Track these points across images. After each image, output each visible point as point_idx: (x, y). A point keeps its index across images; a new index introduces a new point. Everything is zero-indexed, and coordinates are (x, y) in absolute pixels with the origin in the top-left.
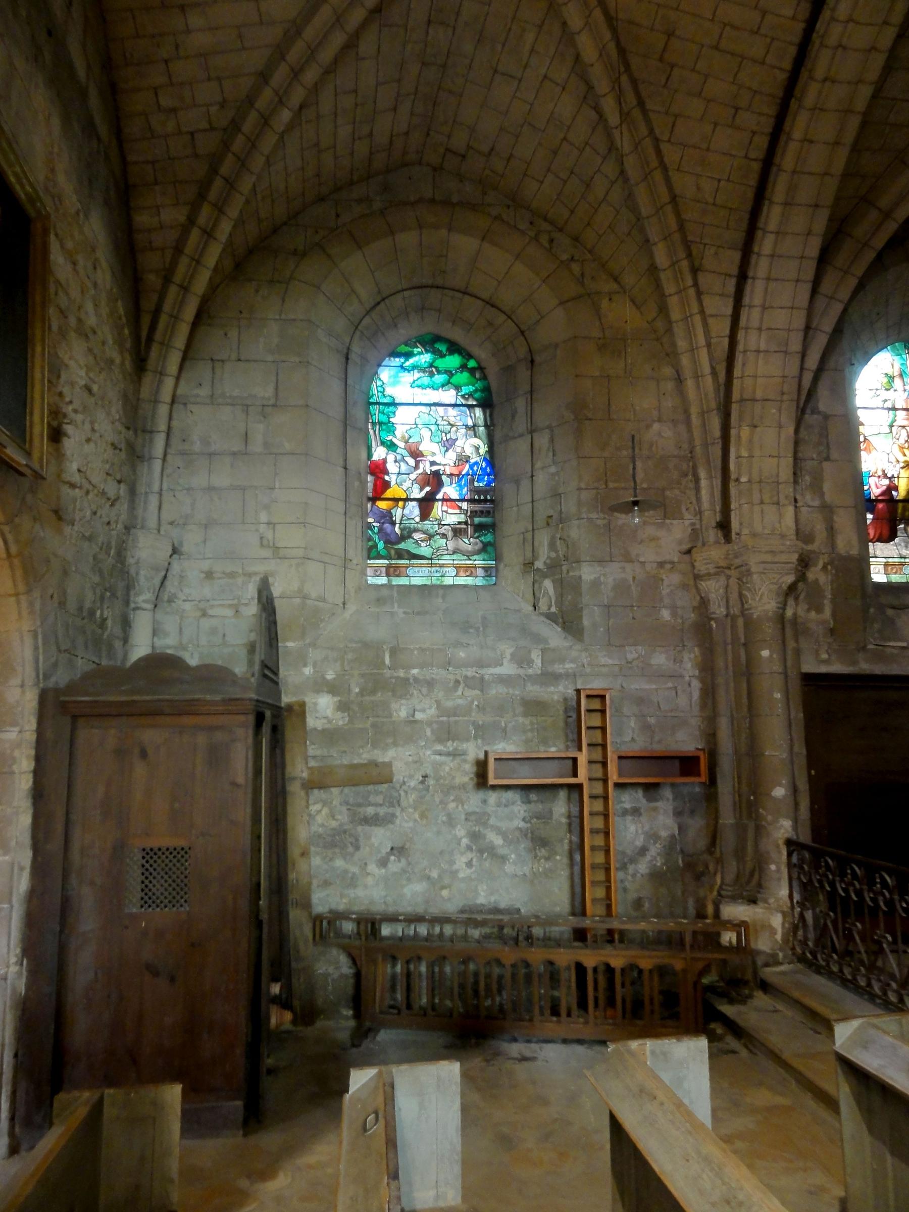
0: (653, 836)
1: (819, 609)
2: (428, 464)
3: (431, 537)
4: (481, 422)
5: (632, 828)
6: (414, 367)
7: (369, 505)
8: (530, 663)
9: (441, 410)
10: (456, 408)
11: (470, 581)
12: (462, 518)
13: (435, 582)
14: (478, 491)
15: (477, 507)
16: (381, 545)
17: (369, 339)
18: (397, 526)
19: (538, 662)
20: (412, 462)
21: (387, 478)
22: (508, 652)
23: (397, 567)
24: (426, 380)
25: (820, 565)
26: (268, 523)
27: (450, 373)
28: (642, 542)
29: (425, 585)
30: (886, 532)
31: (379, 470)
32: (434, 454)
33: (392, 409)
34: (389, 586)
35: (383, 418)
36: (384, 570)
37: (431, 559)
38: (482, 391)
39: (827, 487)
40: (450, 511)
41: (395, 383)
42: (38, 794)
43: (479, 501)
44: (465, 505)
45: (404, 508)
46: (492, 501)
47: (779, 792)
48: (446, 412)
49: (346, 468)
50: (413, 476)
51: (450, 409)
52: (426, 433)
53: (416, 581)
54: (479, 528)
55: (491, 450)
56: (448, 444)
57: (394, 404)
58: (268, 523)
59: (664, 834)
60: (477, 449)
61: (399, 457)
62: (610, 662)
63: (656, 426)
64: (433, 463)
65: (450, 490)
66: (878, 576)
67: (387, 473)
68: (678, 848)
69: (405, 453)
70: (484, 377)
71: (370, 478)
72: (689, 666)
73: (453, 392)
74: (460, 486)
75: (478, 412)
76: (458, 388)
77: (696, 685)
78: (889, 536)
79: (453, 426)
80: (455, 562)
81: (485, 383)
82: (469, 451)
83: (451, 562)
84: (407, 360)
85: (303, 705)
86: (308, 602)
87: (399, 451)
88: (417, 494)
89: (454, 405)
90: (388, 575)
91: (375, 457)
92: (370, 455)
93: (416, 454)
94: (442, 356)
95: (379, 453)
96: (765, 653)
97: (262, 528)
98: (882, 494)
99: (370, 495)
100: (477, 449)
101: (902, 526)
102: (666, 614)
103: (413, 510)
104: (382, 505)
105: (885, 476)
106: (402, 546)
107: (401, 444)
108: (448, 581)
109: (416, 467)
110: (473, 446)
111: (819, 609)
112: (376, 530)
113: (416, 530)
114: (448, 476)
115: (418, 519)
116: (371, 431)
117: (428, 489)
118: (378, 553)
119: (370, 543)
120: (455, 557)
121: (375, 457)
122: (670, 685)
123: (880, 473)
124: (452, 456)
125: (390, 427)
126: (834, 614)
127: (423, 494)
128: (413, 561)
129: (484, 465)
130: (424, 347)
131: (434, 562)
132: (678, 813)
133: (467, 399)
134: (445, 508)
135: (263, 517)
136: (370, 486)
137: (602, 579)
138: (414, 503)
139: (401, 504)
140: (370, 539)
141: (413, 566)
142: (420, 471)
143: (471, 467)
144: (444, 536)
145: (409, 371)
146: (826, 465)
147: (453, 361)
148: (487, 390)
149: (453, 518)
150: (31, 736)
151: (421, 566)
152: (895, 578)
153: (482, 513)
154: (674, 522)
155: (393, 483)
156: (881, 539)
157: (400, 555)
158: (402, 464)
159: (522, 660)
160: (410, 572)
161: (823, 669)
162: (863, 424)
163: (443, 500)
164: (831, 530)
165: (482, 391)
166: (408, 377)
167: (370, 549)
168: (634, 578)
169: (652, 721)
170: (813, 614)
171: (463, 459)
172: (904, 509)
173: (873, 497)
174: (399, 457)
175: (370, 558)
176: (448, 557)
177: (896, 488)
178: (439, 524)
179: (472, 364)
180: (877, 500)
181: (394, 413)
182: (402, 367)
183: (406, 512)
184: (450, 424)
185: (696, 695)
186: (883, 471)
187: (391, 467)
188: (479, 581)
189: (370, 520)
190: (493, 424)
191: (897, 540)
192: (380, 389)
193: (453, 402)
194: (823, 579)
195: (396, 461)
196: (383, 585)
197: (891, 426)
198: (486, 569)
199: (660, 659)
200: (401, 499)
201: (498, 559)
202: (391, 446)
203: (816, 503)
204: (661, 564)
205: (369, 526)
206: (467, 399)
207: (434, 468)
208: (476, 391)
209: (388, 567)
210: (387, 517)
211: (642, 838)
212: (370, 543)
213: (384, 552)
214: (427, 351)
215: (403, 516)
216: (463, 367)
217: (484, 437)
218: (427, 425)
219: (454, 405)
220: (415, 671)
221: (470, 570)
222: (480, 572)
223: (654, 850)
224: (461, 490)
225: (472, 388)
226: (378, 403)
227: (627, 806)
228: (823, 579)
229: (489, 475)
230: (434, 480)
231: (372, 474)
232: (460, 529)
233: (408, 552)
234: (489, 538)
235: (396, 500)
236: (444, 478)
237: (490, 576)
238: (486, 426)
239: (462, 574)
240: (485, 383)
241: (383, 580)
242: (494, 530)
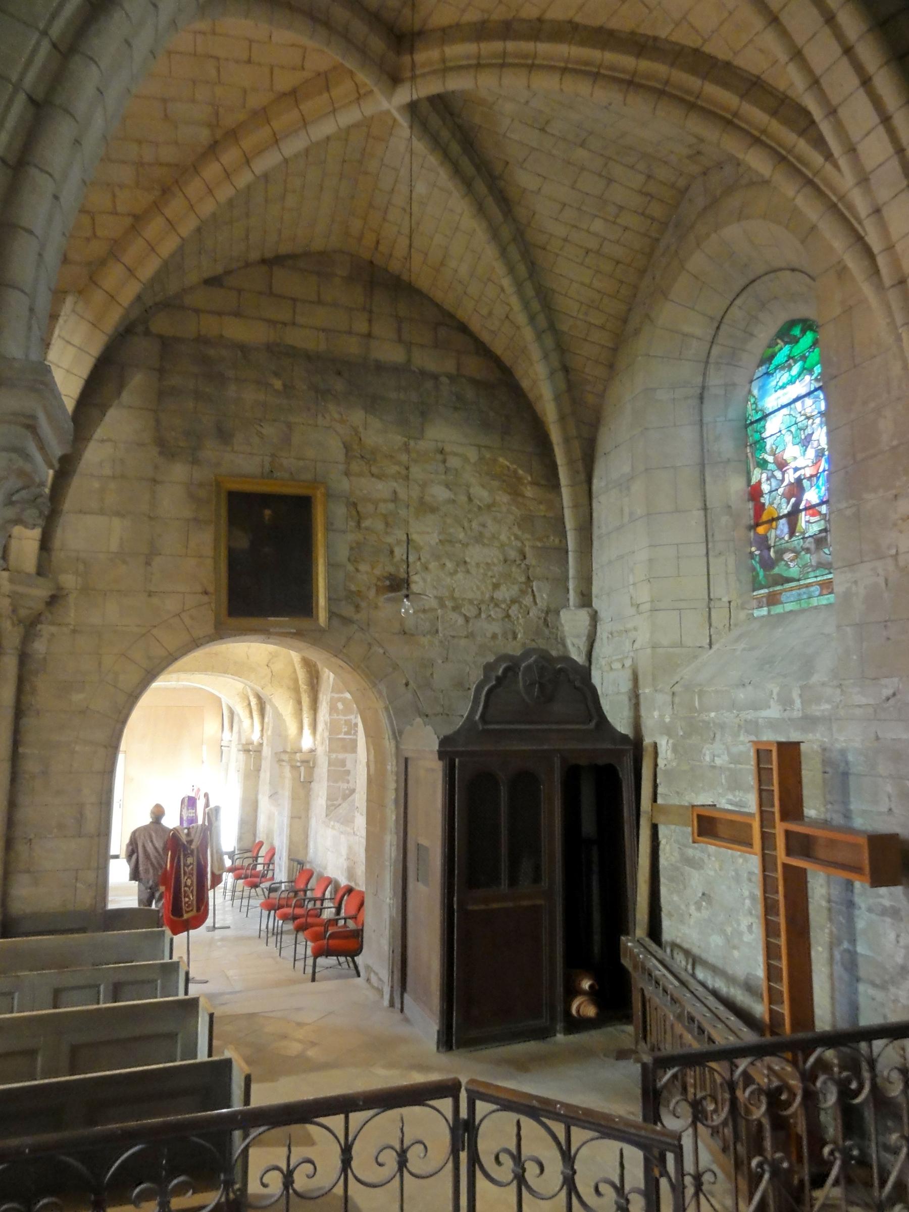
2: (791, 471)
3: (797, 553)
6: (776, 368)
8: (792, 703)
10: (812, 396)
17: (728, 364)
18: (772, 550)
19: (798, 703)
22: (776, 690)
27: (804, 358)
37: (799, 580)
40: (813, 519)
50: (781, 491)
51: (806, 399)
62: (864, 701)
64: (796, 469)
65: (812, 496)
74: (818, 487)
80: (819, 579)
83: (815, 580)
86: (660, 651)
104: (761, 530)
107: (770, 459)
109: (783, 480)
112: (757, 559)
115: (786, 538)
117: (793, 500)
118: (760, 584)
120: (818, 573)
127: (789, 508)
131: (802, 582)
134: (808, 518)
137: (854, 589)
141: (785, 590)
144: (808, 550)
151: (791, 589)
158: (772, 480)
159: (786, 702)
163: (806, 509)
168: (886, 581)
175: (754, 591)
176: (812, 574)
178: (803, 538)
187: (765, 488)
189: (753, 549)
192: (754, 406)
215: (776, 537)
220: (713, 714)
227: (887, 903)
232: (822, 538)
233: (780, 576)
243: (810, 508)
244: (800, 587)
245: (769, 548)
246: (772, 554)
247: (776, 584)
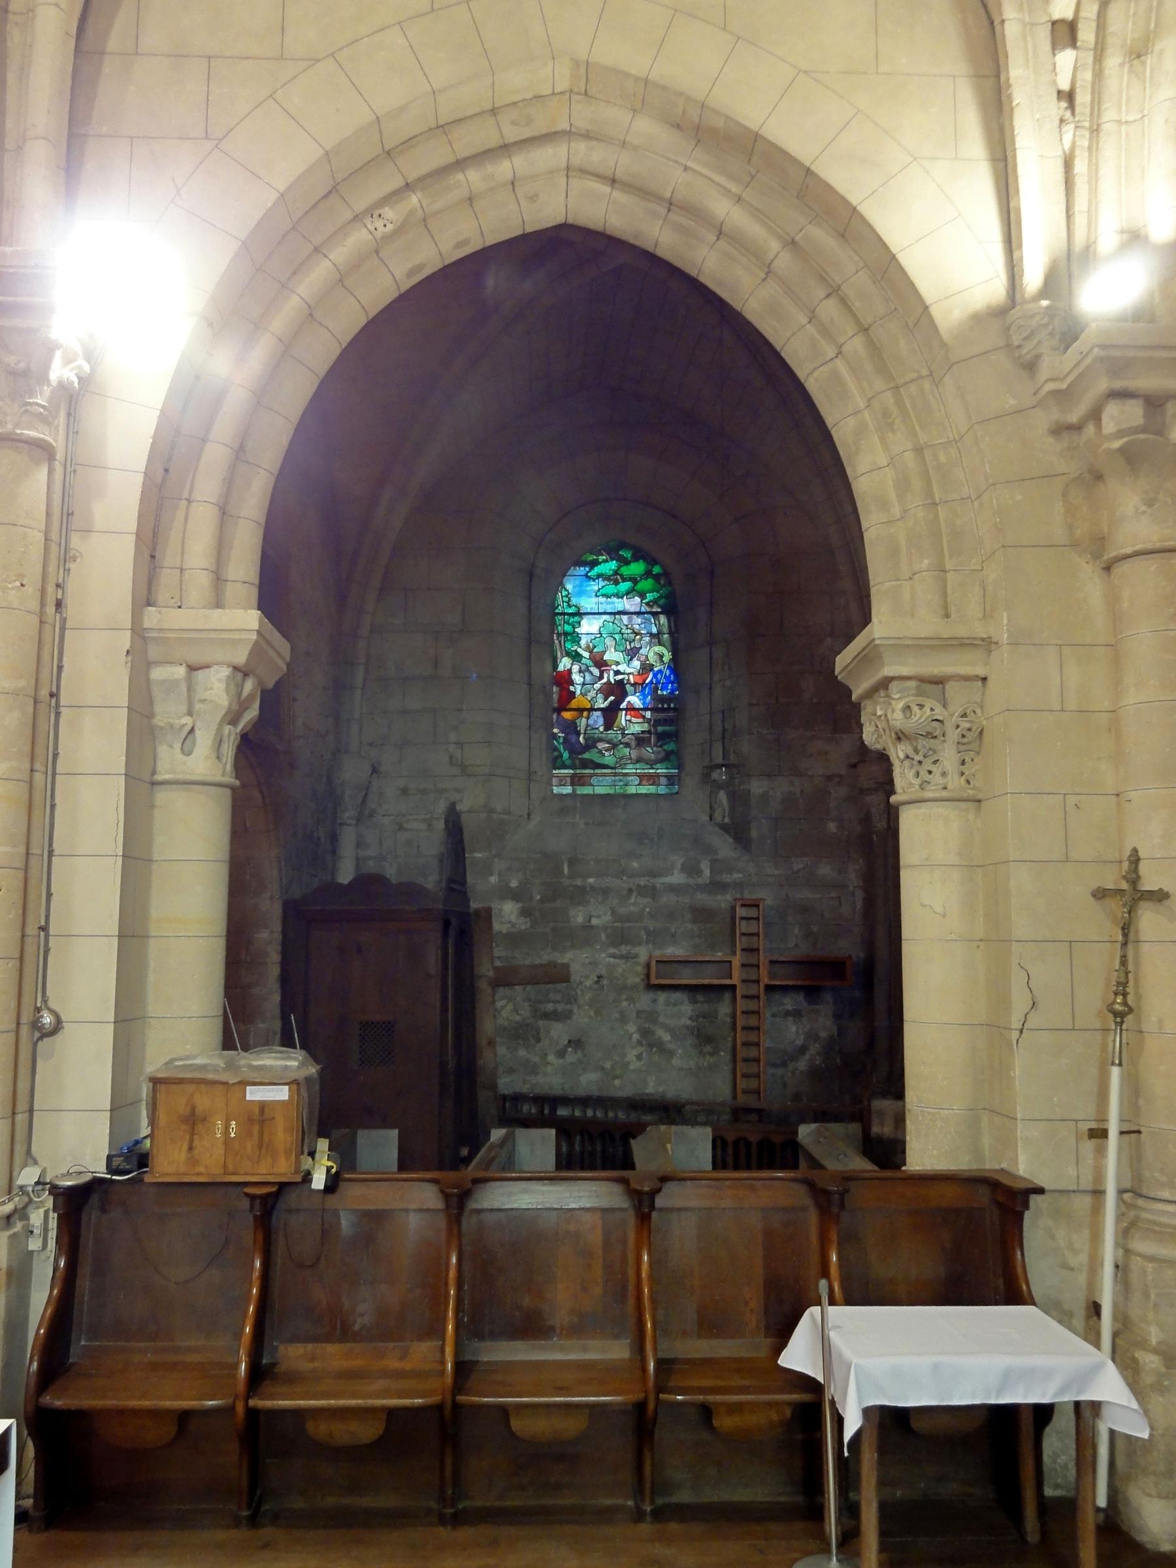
0: (812, 1036)
3: (614, 746)
4: (666, 629)
5: (794, 1029)
6: (599, 576)
7: (555, 716)
8: (699, 872)
9: (625, 618)
11: (652, 789)
12: (646, 727)
13: (619, 790)
14: (662, 699)
15: (661, 716)
16: (566, 755)
19: (707, 872)
20: (596, 672)
21: (572, 688)
22: (680, 862)
23: (582, 776)
24: (611, 589)
26: (457, 743)
27: (634, 581)
28: (811, 755)
29: (608, 795)
31: (565, 680)
32: (618, 663)
33: (576, 619)
34: (573, 795)
35: (568, 628)
36: (569, 780)
37: (614, 768)
38: (666, 597)
40: (634, 720)
41: (581, 593)
42: (284, 980)
43: (663, 710)
44: (648, 714)
45: (588, 718)
46: (675, 709)
48: (630, 620)
49: (529, 684)
50: (597, 686)
51: (635, 617)
52: (609, 642)
53: (600, 790)
54: (662, 737)
55: (675, 659)
56: (632, 653)
57: (579, 614)
58: (457, 743)
59: (823, 1034)
60: (661, 656)
61: (583, 668)
62: (776, 872)
63: (828, 641)
64: (617, 673)
65: (634, 700)
67: (572, 683)
68: (837, 1048)
69: (589, 663)
70: (669, 583)
71: (555, 689)
72: (853, 878)
73: (637, 599)
75: (663, 619)
76: (642, 595)
77: (860, 895)
79: (637, 634)
81: (669, 589)
82: (652, 659)
84: (592, 569)
85: (489, 911)
86: (495, 816)
87: (584, 661)
88: (601, 703)
89: (638, 613)
90: (572, 784)
91: (561, 668)
92: (555, 666)
93: (601, 664)
94: (626, 562)
95: (564, 663)
97: (452, 748)
99: (556, 705)
100: (661, 656)
102: (832, 827)
103: (597, 719)
104: (567, 715)
106: (586, 756)
108: (632, 790)
109: (601, 677)
110: (656, 654)
112: (561, 740)
113: (601, 740)
114: (632, 685)
115: (601, 729)
116: (556, 642)
117: (612, 698)
118: (563, 762)
119: (556, 754)
120: (638, 766)
121: (561, 668)
122: (834, 894)
124: (636, 664)
125: (576, 638)
127: (607, 703)
128: (598, 771)
129: (668, 673)
130: (609, 554)
132: (838, 1016)
133: (651, 607)
134: (628, 717)
135: (453, 737)
136: (555, 697)
137: (771, 793)
138: (599, 713)
139: (585, 714)
140: (556, 749)
141: (594, 775)
142: (605, 680)
143: (655, 676)
144: (627, 745)
145: (594, 580)
147: (637, 568)
148: (671, 596)
149: (636, 728)
150: (278, 936)
151: (604, 775)
153: (665, 722)
154: (844, 736)
155: (578, 692)
157: (586, 764)
159: (692, 869)
160: (594, 780)
163: (627, 710)
165: (666, 597)
166: (594, 586)
167: (555, 759)
168: (802, 792)
169: (815, 929)
171: (646, 668)
174: (583, 668)
175: (555, 769)
176: (631, 766)
179: (657, 570)
181: (579, 623)
182: (586, 576)
183: (591, 722)
184: (634, 632)
185: (859, 905)
187: (577, 678)
188: (662, 790)
189: (555, 730)
190: (677, 632)
192: (566, 599)
193: (638, 610)
195: (580, 671)
196: (567, 795)
198: (669, 777)
199: (825, 870)
200: (586, 709)
201: (680, 767)
202: (576, 657)
204: (829, 778)
205: (554, 736)
206: (651, 607)
207: (620, 677)
208: (660, 598)
209: (573, 777)
210: (571, 728)
211: (802, 1037)
212: (556, 754)
213: (568, 762)
214: (612, 559)
215: (587, 725)
216: (648, 574)
217: (668, 644)
218: (611, 635)
219: (638, 613)
220: (591, 880)
221: (653, 779)
222: (663, 780)
223: (814, 1049)
224: (645, 697)
225: (656, 595)
226: (564, 614)
227: (790, 1008)
229: (672, 683)
230: (618, 690)
231: (558, 684)
233: (592, 761)
234: (671, 746)
235: (581, 710)
236: (628, 687)
237: (672, 784)
238: (670, 633)
239: (644, 782)
240: (669, 589)
241: (568, 790)
242: (677, 737)
243: (631, 709)
244: (615, 775)
245: (579, 734)
246: (581, 739)
247: (585, 767)
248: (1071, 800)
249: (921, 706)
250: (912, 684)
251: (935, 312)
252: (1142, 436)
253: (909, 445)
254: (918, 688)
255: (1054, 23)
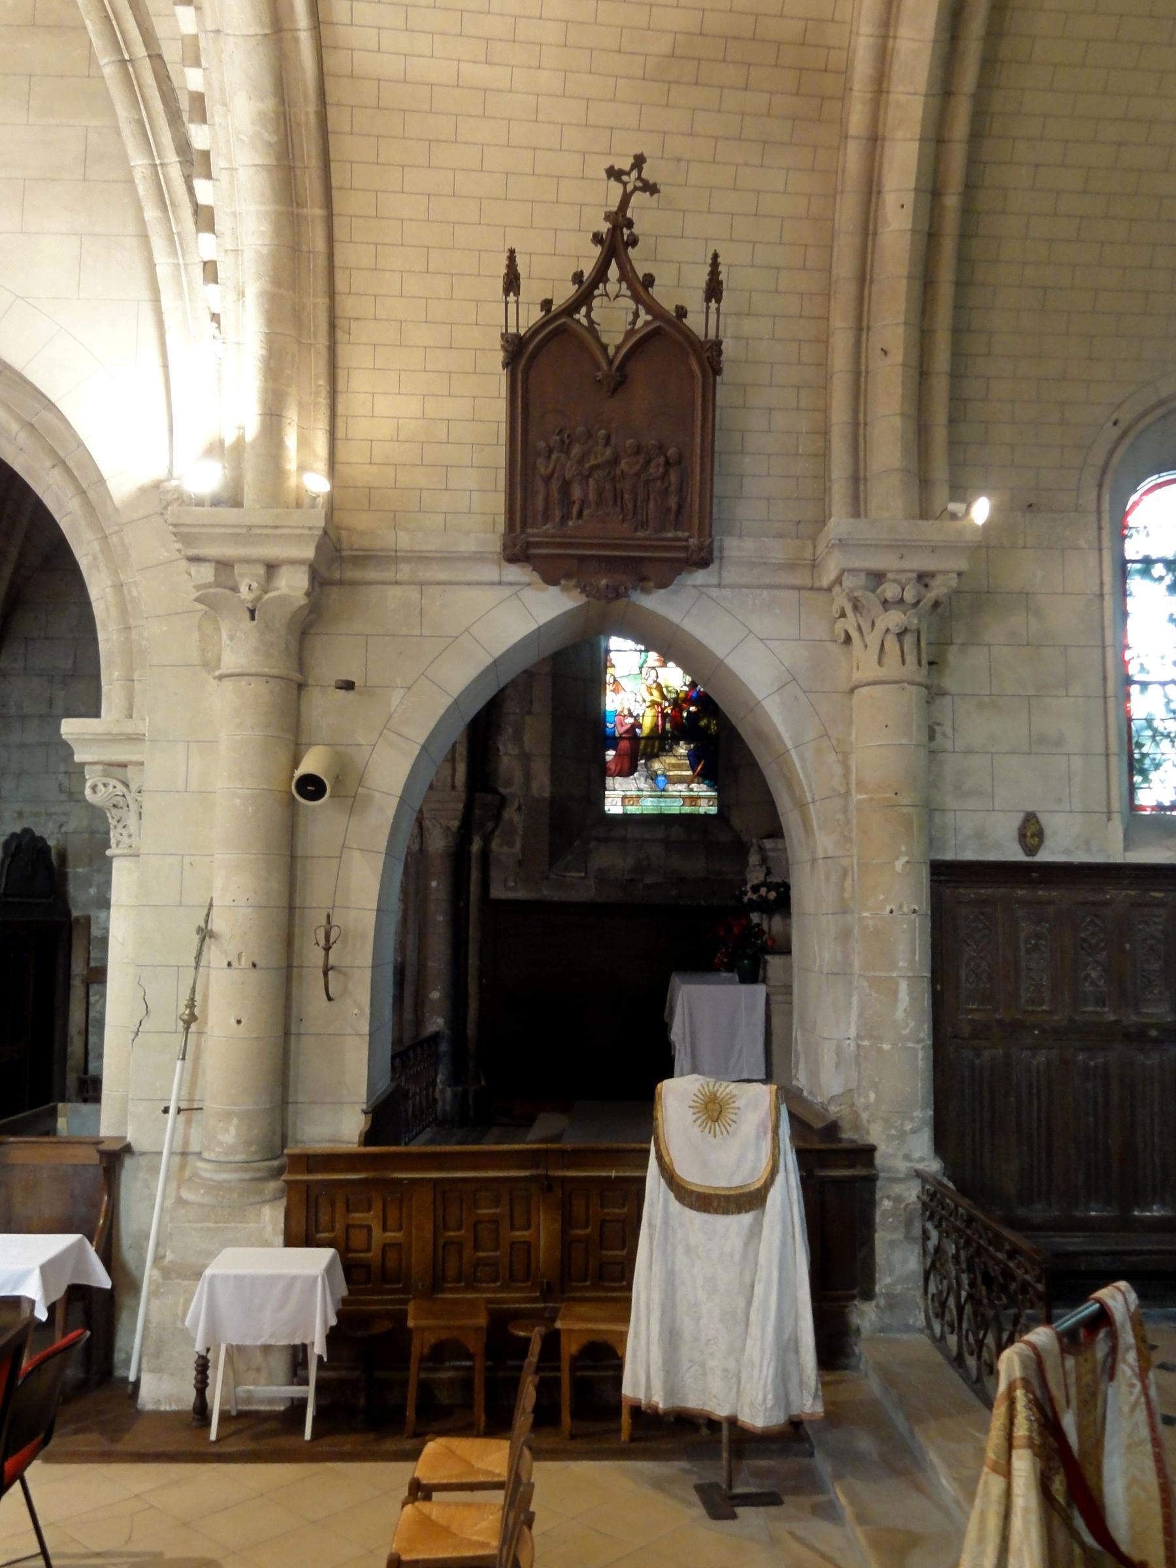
1: (511, 844)
25: (516, 805)
26: (66, 773)
30: (626, 766)
39: (526, 738)
47: (435, 995)
58: (66, 773)
66: (613, 806)
78: (628, 771)
85: (88, 919)
86: (98, 836)
96: (434, 884)
97: (61, 777)
98: (626, 732)
101: (643, 761)
105: (631, 715)
111: (511, 844)
123: (626, 712)
126: (523, 849)
135: (62, 768)
146: (528, 719)
152: (632, 809)
156: (621, 774)
161: (511, 895)
162: (613, 666)
164: (528, 777)
170: (505, 849)
172: (646, 746)
173: (617, 735)
177: (640, 726)
180: (621, 738)
186: (629, 710)
191: (636, 774)
194: (516, 818)
197: (641, 668)
203: (516, 752)
228: (516, 818)
248: (187, 860)
249: (105, 785)
250: (99, 767)
251: (111, 485)
252: (212, 590)
253: (109, 583)
254: (104, 770)
255: (205, 263)
